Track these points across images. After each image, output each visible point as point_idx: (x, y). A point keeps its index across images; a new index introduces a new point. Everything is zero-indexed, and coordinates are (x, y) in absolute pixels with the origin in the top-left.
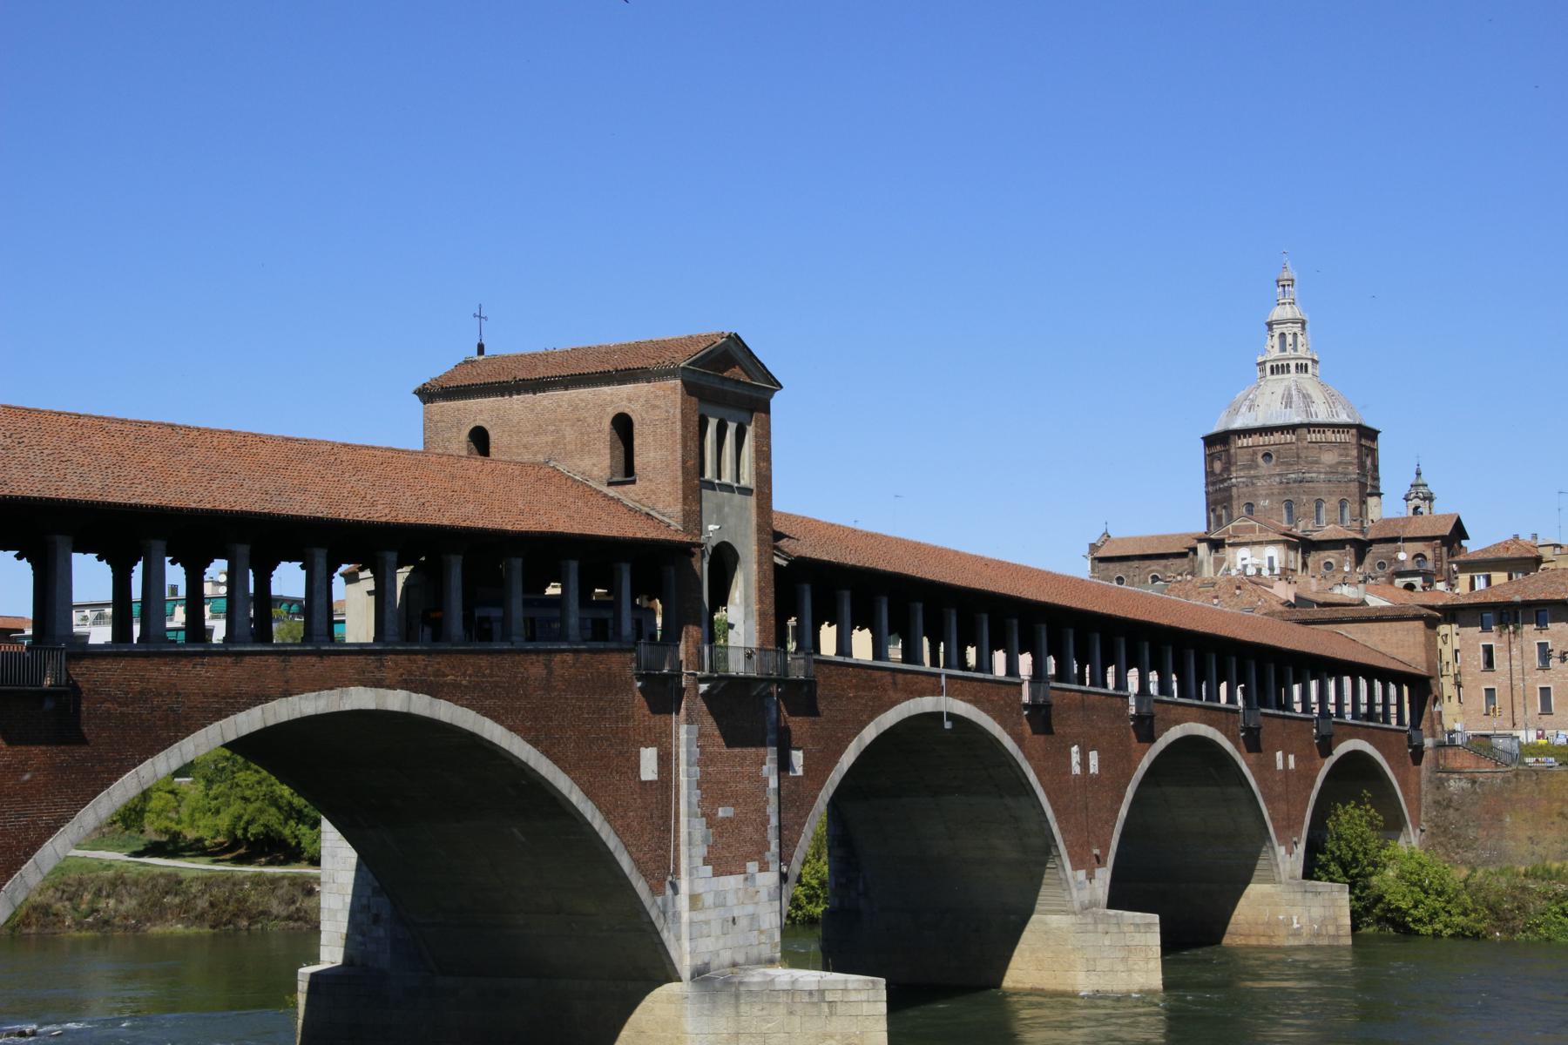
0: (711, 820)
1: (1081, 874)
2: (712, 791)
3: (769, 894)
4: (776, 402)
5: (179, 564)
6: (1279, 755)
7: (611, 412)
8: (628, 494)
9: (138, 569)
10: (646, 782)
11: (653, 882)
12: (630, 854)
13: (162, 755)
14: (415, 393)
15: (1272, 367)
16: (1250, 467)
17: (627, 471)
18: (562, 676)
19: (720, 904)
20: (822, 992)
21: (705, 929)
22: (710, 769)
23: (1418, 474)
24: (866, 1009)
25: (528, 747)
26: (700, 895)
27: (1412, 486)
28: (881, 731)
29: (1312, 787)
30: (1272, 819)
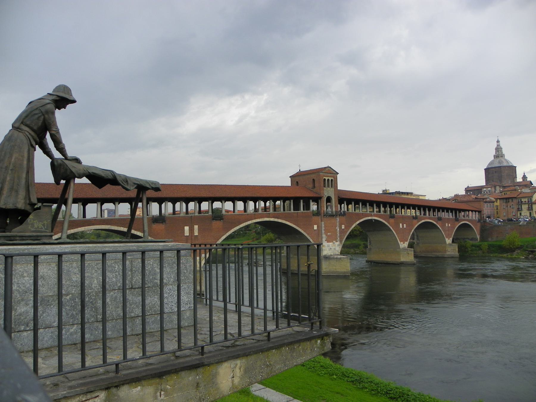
2: (326, 231)
3: (338, 246)
4: (338, 176)
6: (447, 224)
7: (312, 179)
8: (315, 190)
12: (312, 240)
15: (496, 157)
17: (314, 187)
19: (328, 246)
21: (325, 250)
23: (524, 174)
24: (347, 261)
26: (324, 245)
29: (454, 229)
30: (445, 234)
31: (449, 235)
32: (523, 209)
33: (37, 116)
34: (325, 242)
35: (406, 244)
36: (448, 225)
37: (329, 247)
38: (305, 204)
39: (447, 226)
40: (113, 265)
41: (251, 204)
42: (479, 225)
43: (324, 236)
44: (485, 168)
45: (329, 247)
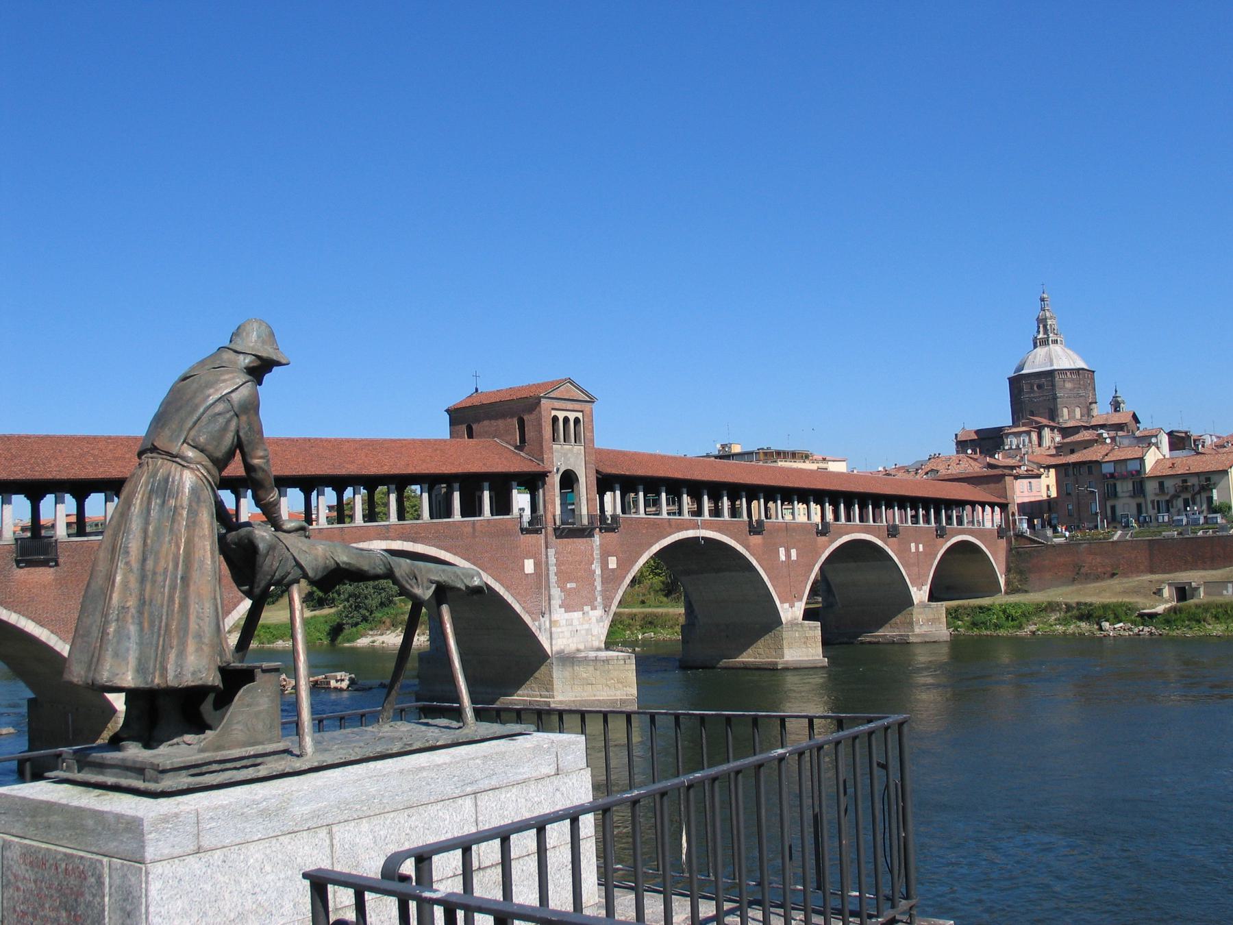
0: (563, 589)
2: (563, 577)
3: (597, 620)
6: (913, 545)
9: (314, 494)
10: (527, 574)
11: (533, 616)
12: (520, 604)
14: (446, 411)
16: (1030, 393)
18: (482, 531)
20: (608, 660)
22: (562, 568)
23: (1116, 391)
26: (555, 621)
27: (1114, 397)
28: (661, 547)
31: (919, 578)
32: (1120, 494)
33: (221, 420)
34: (558, 609)
35: (800, 607)
36: (917, 548)
37: (572, 625)
38: (493, 493)
39: (913, 550)
40: (441, 814)
41: (330, 496)
42: (1003, 543)
43: (556, 592)
44: (1012, 375)
45: (572, 625)
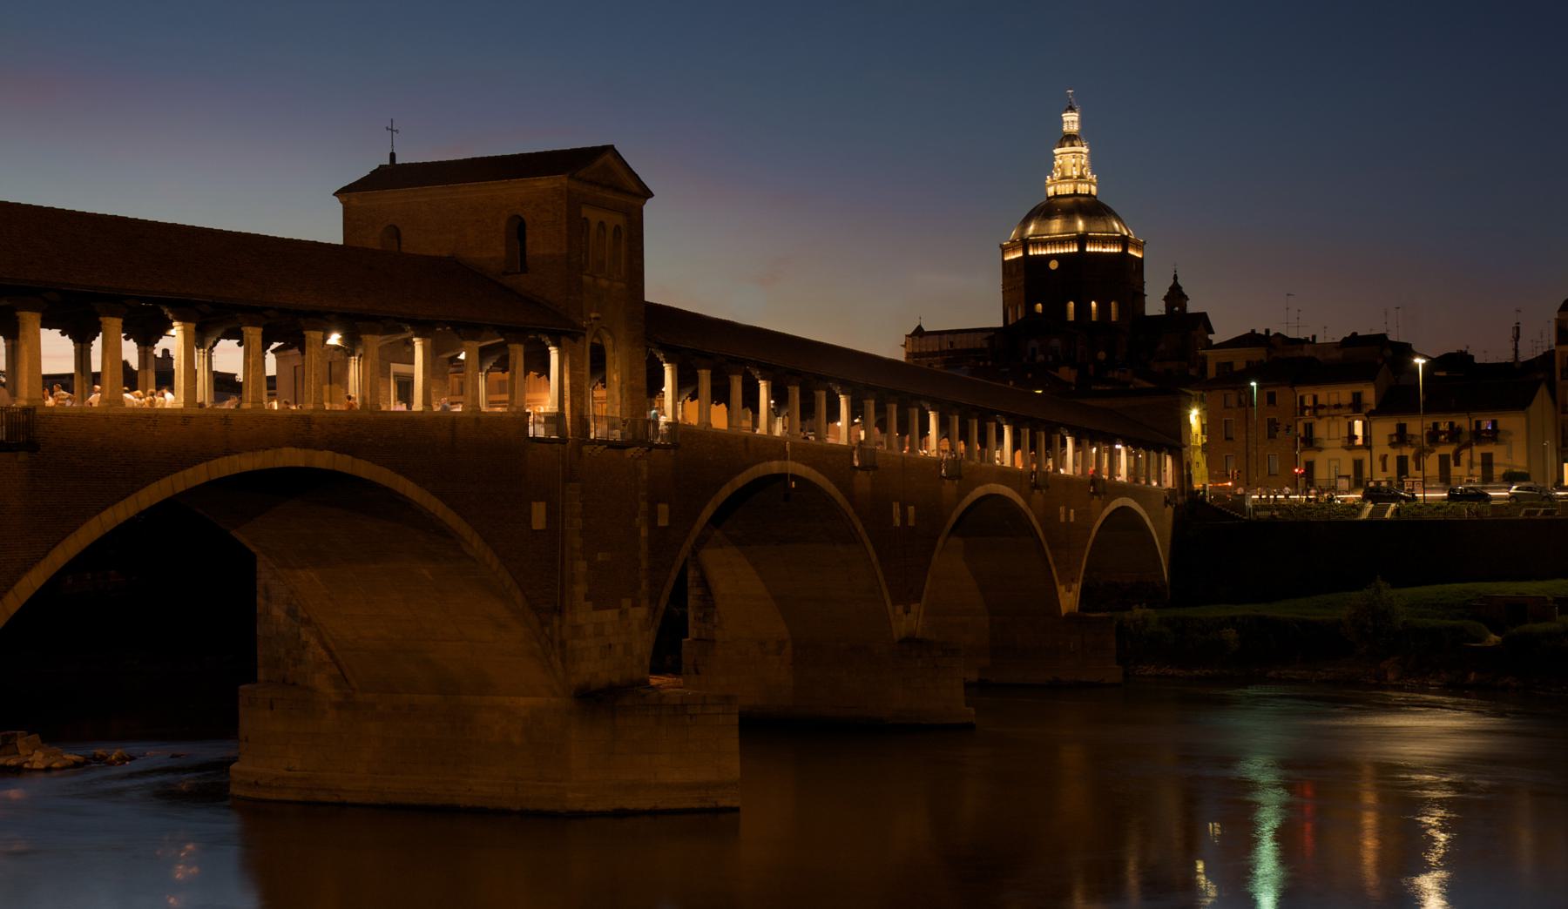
1: (900, 609)
4: (649, 208)
5: (131, 340)
6: (1062, 509)
9: (97, 345)
10: (536, 531)
13: (122, 504)
14: (334, 195)
23: (1175, 277)
25: (435, 500)
